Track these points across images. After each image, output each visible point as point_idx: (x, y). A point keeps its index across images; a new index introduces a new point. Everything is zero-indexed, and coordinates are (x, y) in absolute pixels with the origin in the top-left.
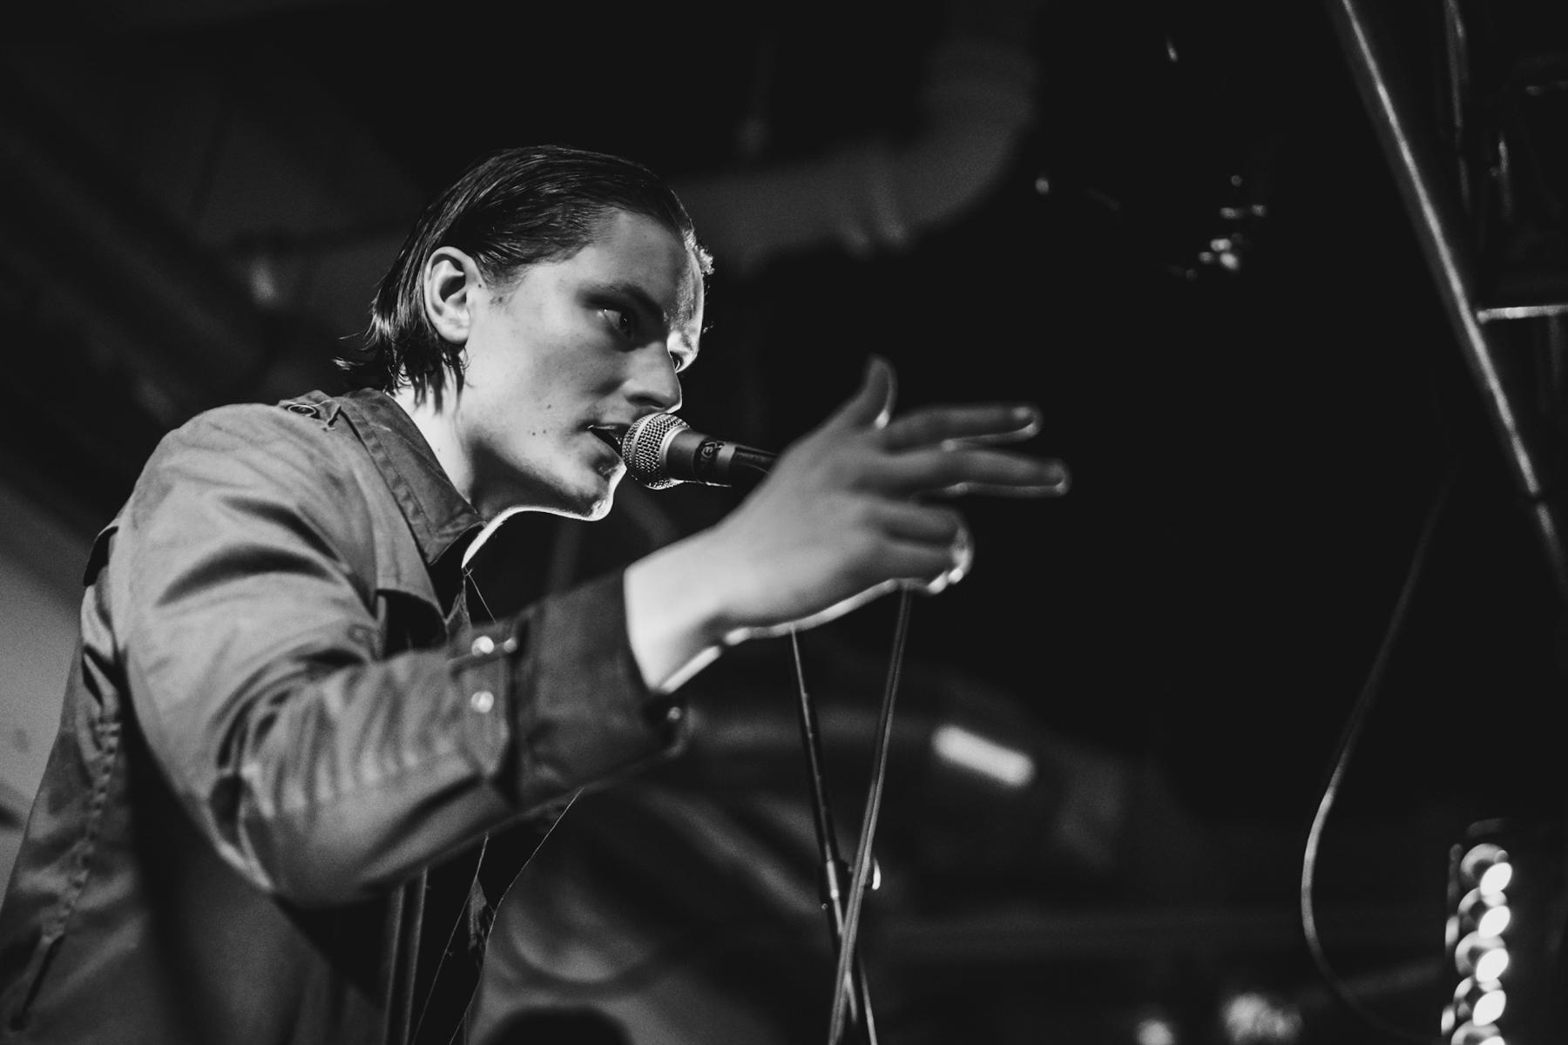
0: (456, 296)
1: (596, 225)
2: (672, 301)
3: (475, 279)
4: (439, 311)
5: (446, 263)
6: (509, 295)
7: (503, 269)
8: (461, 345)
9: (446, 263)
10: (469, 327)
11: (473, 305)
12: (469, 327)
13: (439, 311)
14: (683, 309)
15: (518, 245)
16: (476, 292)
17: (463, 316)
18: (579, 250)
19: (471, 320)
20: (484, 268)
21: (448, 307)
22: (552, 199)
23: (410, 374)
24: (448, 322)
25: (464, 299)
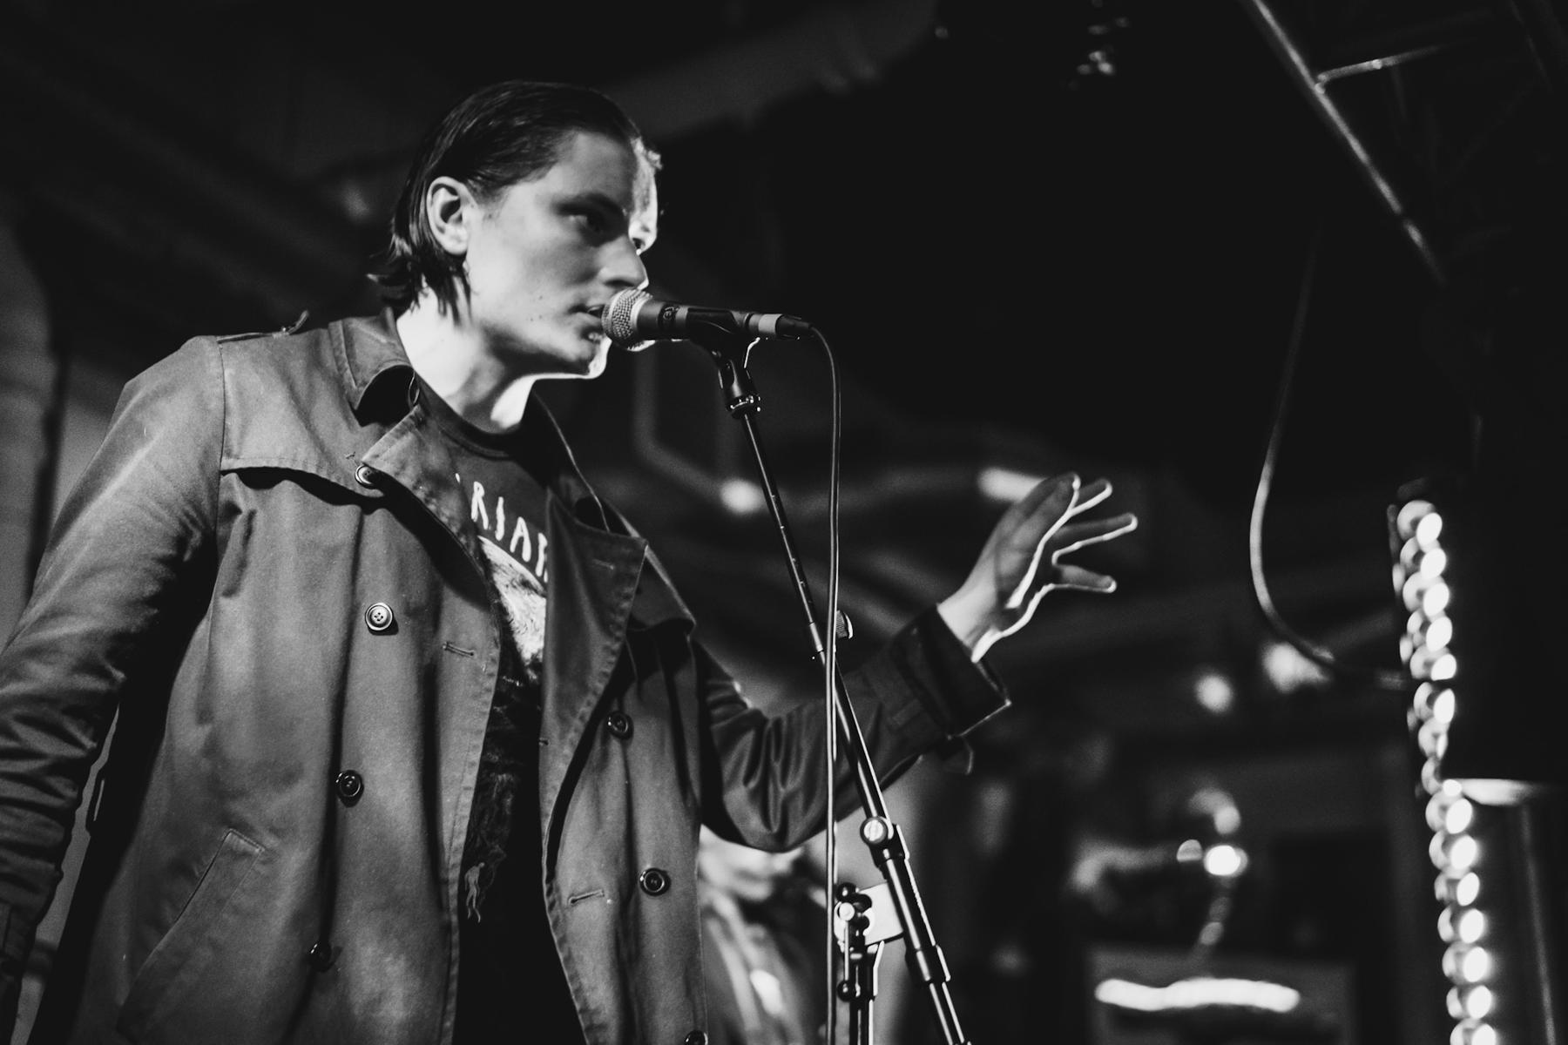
0: (455, 216)
1: (560, 147)
2: (628, 200)
3: (467, 201)
4: (442, 230)
5: (442, 191)
6: (497, 211)
7: (490, 190)
8: (462, 257)
9: (442, 191)
10: (468, 241)
11: (468, 223)
12: (468, 241)
13: (442, 230)
14: (638, 203)
15: (499, 170)
16: (471, 211)
17: (461, 231)
18: (550, 168)
19: (470, 235)
20: (473, 191)
21: (450, 227)
22: (521, 131)
23: (430, 284)
24: (450, 238)
25: (460, 218)
